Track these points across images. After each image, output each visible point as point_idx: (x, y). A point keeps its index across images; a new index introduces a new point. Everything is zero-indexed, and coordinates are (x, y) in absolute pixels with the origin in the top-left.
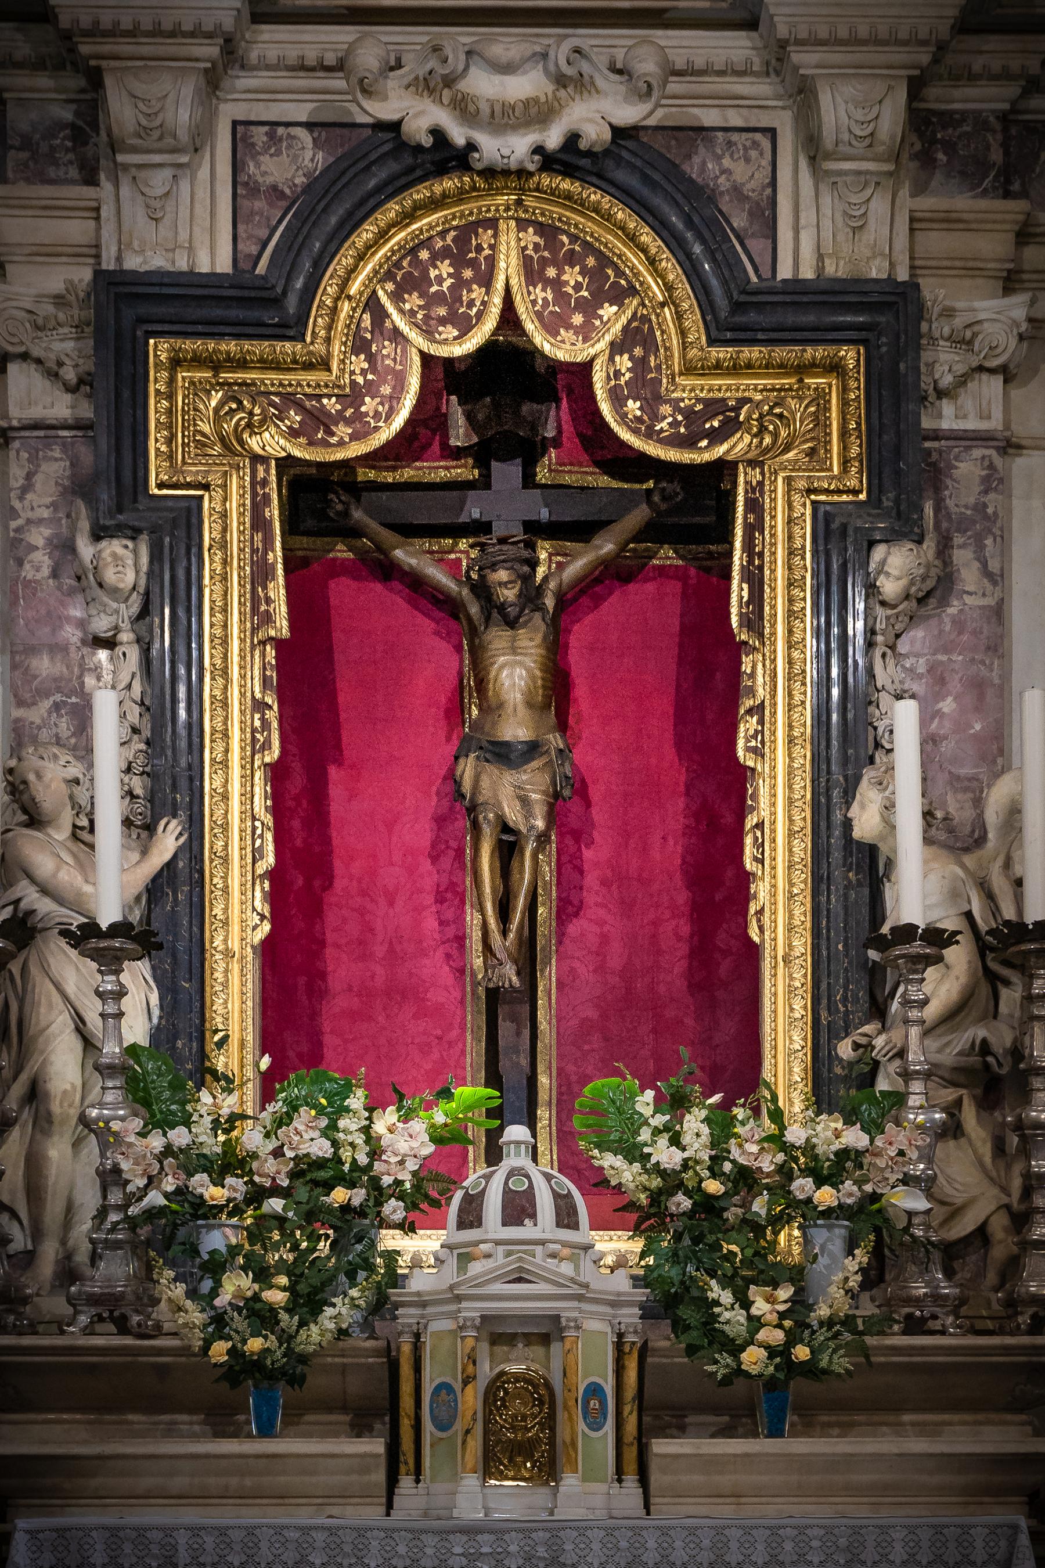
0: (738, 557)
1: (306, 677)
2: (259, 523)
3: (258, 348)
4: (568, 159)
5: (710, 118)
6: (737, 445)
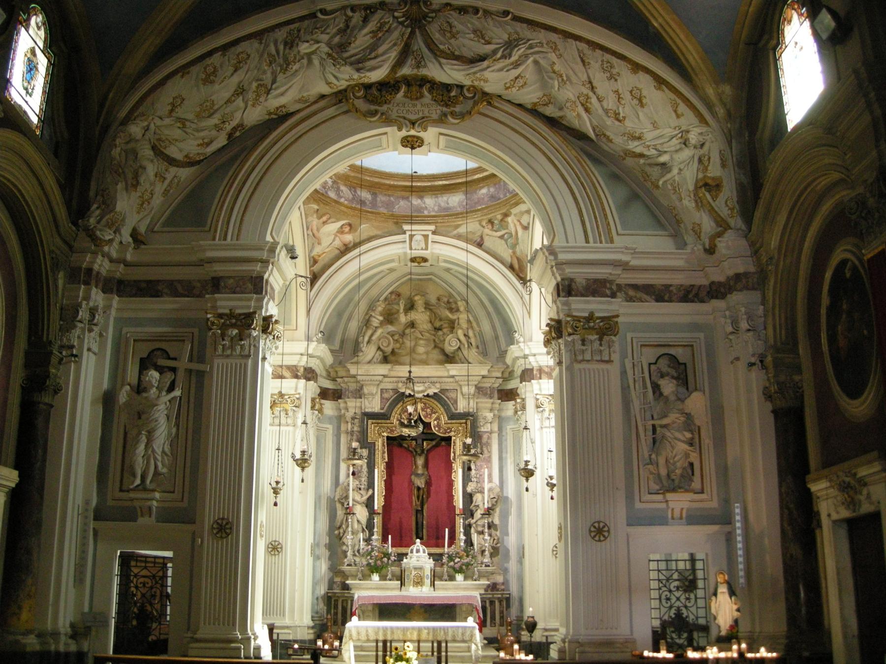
1: (390, 467)
2: (383, 445)
3: (383, 421)
4: (428, 396)
6: (452, 434)
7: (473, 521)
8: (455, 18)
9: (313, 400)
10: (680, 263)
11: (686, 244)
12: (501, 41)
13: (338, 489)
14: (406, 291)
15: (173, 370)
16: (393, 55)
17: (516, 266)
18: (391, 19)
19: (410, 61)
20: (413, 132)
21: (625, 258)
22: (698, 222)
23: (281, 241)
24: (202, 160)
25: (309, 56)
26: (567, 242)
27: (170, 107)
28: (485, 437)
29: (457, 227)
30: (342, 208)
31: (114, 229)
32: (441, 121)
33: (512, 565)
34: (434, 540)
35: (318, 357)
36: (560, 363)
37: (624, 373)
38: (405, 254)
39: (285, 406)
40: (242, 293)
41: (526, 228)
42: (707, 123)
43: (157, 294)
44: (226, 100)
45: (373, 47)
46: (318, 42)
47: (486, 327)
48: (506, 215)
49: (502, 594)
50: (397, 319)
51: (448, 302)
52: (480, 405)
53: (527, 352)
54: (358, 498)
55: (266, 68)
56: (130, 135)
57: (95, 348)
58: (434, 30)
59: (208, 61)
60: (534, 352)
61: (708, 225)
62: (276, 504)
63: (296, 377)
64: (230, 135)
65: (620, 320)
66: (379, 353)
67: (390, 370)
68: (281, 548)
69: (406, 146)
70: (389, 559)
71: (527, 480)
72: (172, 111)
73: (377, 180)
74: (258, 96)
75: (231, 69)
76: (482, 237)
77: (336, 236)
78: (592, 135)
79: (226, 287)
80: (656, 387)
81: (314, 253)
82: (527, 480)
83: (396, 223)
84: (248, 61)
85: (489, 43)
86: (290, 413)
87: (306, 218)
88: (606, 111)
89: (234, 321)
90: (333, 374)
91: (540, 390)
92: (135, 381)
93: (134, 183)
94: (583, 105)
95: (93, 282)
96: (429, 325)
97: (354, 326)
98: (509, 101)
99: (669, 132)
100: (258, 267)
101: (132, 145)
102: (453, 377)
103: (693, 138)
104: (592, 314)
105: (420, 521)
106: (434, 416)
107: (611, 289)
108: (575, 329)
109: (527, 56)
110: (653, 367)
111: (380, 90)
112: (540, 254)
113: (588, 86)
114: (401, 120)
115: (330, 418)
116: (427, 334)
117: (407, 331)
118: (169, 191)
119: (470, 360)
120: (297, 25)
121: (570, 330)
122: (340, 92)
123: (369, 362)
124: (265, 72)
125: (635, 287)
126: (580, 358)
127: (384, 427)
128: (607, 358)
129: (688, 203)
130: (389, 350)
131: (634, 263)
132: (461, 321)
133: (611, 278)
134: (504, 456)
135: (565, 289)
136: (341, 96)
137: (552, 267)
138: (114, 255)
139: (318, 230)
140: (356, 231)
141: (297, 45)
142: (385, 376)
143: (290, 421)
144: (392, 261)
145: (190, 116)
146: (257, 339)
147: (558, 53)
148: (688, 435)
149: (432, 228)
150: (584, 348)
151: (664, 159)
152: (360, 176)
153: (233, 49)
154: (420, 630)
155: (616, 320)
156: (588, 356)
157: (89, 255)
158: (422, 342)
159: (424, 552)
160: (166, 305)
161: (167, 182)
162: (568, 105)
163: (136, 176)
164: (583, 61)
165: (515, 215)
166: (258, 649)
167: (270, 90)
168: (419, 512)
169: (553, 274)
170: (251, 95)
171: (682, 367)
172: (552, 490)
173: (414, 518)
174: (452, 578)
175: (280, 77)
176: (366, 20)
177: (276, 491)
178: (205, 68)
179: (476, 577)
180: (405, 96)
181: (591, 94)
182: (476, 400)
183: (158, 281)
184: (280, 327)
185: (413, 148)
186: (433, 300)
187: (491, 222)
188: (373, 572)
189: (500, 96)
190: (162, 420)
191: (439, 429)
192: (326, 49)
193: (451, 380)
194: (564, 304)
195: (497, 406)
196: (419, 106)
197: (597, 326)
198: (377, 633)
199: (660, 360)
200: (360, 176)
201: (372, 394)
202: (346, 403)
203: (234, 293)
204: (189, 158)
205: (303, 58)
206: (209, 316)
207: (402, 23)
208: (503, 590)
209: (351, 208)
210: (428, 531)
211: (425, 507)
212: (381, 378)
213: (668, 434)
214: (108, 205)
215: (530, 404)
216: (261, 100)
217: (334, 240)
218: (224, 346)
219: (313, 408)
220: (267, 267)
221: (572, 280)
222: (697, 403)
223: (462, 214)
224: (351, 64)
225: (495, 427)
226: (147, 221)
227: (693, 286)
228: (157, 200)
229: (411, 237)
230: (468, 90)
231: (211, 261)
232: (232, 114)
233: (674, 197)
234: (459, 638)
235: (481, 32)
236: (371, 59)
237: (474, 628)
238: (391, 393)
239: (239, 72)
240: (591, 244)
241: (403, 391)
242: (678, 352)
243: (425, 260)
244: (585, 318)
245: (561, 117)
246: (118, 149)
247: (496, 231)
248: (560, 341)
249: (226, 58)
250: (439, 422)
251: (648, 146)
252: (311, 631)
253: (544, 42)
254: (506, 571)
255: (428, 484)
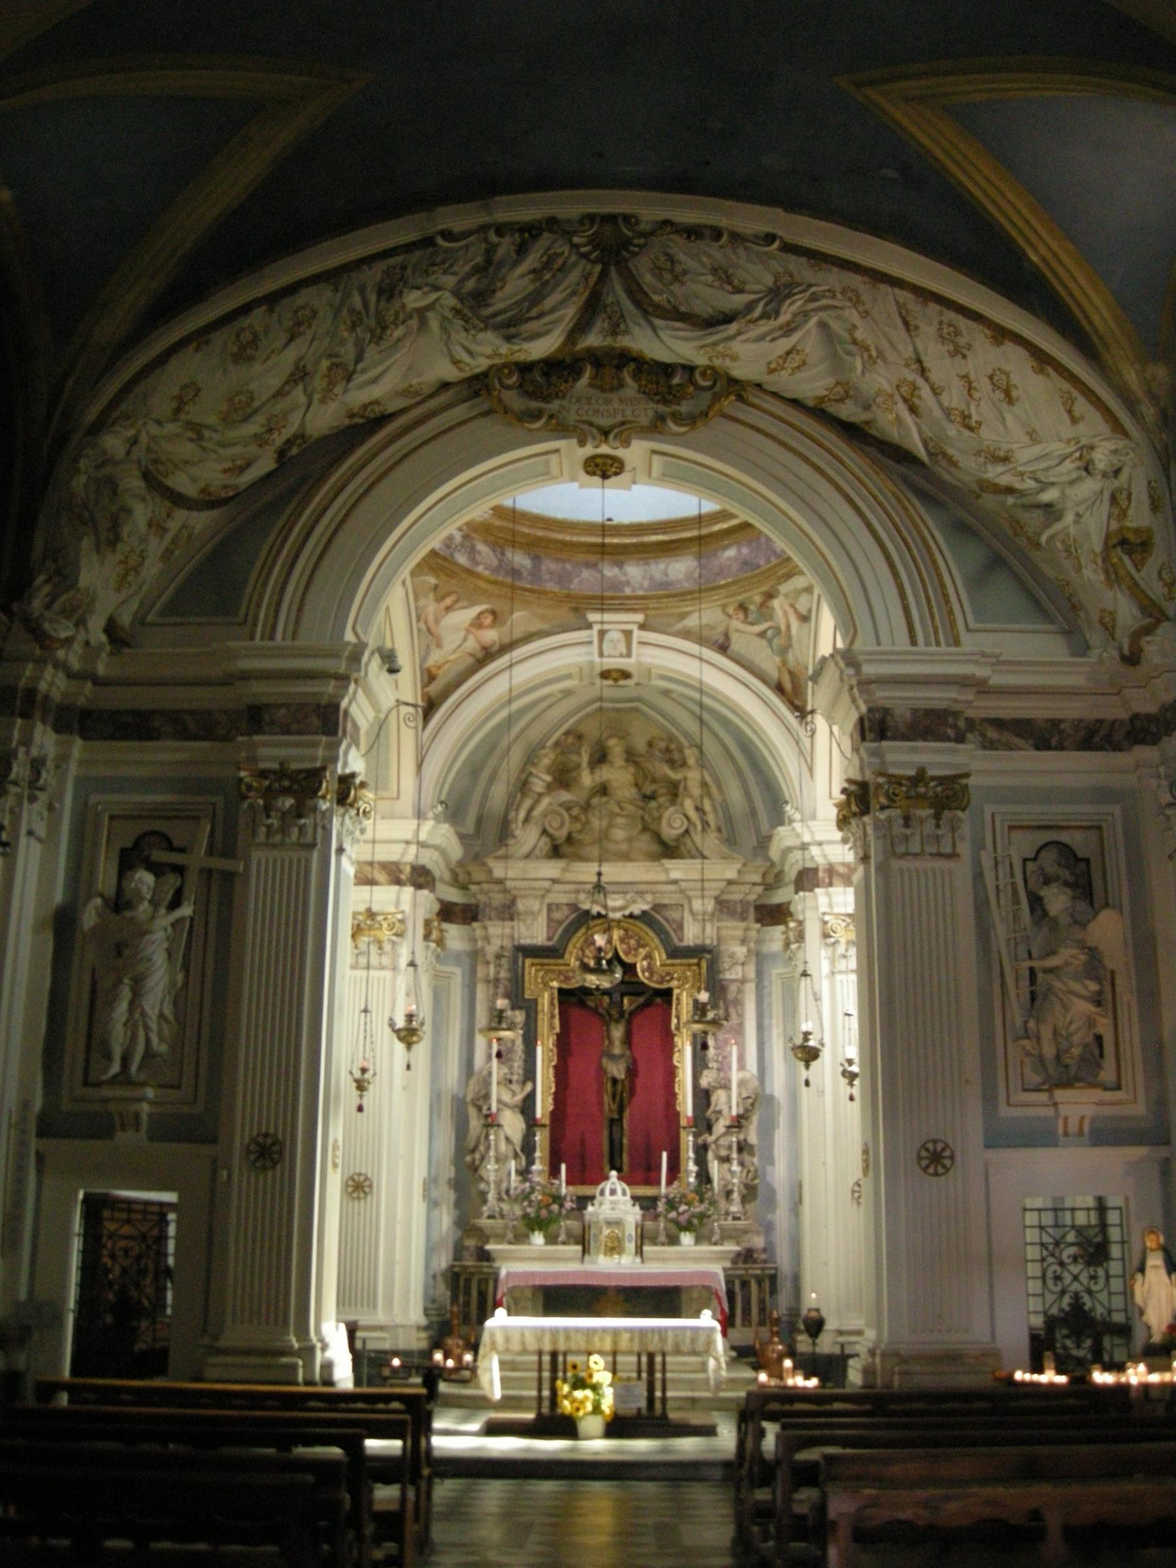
0: (674, 1012)
1: (563, 1044)
2: (552, 1004)
3: (552, 961)
4: (631, 916)
5: (666, 902)
6: (674, 984)
7: (711, 1139)
8: (679, 246)
9: (427, 923)
10: (1076, 680)
11: (1088, 648)
12: (760, 287)
13: (472, 1082)
14: (592, 731)
15: (180, 870)
16: (570, 312)
17: (788, 686)
18: (566, 250)
19: (601, 323)
20: (605, 449)
21: (980, 672)
22: (1110, 608)
23: (372, 642)
24: (232, 498)
25: (421, 312)
26: (879, 644)
27: (175, 405)
28: (733, 989)
29: (683, 616)
30: (481, 583)
31: (75, 617)
32: (656, 428)
33: (781, 1217)
34: (641, 1172)
35: (436, 848)
36: (865, 859)
37: (978, 876)
38: (591, 663)
39: (378, 933)
40: (301, 733)
41: (805, 619)
42: (1125, 433)
43: (149, 734)
44: (273, 390)
45: (535, 298)
46: (436, 288)
47: (735, 794)
48: (770, 596)
49: (763, 1269)
50: (576, 780)
51: (668, 750)
52: (724, 932)
53: (807, 838)
54: (507, 1097)
55: (345, 334)
56: (105, 453)
57: (41, 831)
58: (643, 268)
59: (245, 322)
60: (819, 837)
61: (1127, 613)
62: (360, 1109)
63: (398, 882)
64: (281, 454)
65: (971, 781)
66: (545, 839)
67: (564, 870)
68: (371, 1186)
69: (593, 474)
70: (561, 1206)
71: (807, 1067)
72: (178, 411)
73: (541, 533)
74: (332, 383)
75: (284, 337)
76: (726, 635)
77: (468, 632)
78: (922, 454)
79: (272, 722)
80: (1036, 902)
81: (430, 662)
82: (807, 1067)
83: (576, 610)
84: (315, 323)
85: (739, 291)
86: (387, 947)
87: (416, 599)
88: (947, 412)
89: (286, 783)
90: (462, 877)
91: (831, 905)
92: (111, 891)
93: (112, 538)
94: (905, 400)
95: (38, 714)
96: (634, 790)
97: (499, 792)
98: (775, 394)
99: (1057, 448)
100: (331, 687)
101: (107, 471)
102: (675, 882)
103: (1101, 458)
104: (922, 771)
105: (616, 1137)
106: (642, 952)
107: (955, 727)
108: (892, 798)
109: (805, 315)
110: (1030, 866)
111: (546, 374)
112: (831, 665)
113: (915, 367)
114: (585, 427)
115: (457, 958)
116: (631, 807)
117: (595, 801)
118: (172, 553)
119: (706, 853)
120: (399, 259)
121: (883, 800)
122: (476, 377)
123: (527, 856)
124: (343, 342)
125: (999, 724)
126: (901, 849)
127: (553, 971)
128: (948, 849)
129: (1092, 574)
130: (562, 834)
131: (997, 680)
132: (690, 784)
133: (956, 707)
134: (766, 1022)
135: (875, 728)
136: (477, 386)
137: (851, 688)
138: (75, 664)
139: (437, 621)
140: (505, 622)
141: (401, 293)
142: (554, 881)
143: (386, 961)
144: (568, 676)
145: (212, 420)
146: (327, 816)
147: (861, 308)
148: (1093, 987)
149: (639, 617)
150: (908, 831)
151: (1048, 496)
152: (510, 525)
153: (285, 302)
154: (616, 1332)
155: (964, 781)
156: (915, 847)
157: (30, 666)
158: (620, 821)
159: (624, 1193)
160: (165, 755)
161: (169, 537)
162: (880, 400)
163: (115, 527)
164: (906, 323)
165: (786, 595)
166: (328, 1366)
167: (354, 372)
168: (615, 1123)
169: (854, 700)
170: (318, 383)
171: (1082, 865)
172: (851, 1084)
173: (606, 1133)
174: (673, 1240)
175: (371, 351)
176: (522, 250)
177: (361, 1086)
178: (238, 336)
179: (716, 1238)
180: (591, 385)
181: (920, 382)
182: (717, 924)
183: (154, 712)
184: (368, 794)
185: (605, 476)
186: (640, 745)
187: (743, 607)
188: (533, 1230)
189: (759, 386)
190: (159, 959)
191: (652, 974)
192: (450, 301)
193: (672, 888)
194: (874, 753)
195: (753, 934)
196: (616, 404)
197: (931, 794)
198: (540, 1339)
199: (1044, 854)
200: (510, 525)
201: (532, 913)
202: (485, 928)
203: (288, 732)
204: (210, 494)
205: (411, 317)
206: (243, 774)
207: (585, 256)
208: (765, 1261)
209: (495, 583)
210: (630, 1156)
211: (626, 1114)
212: (547, 884)
213: (1058, 985)
214: (64, 577)
215: (812, 931)
216: (336, 390)
217: (465, 639)
218: (269, 827)
219: (427, 937)
220: (346, 688)
221: (886, 712)
222: (1108, 929)
223: (690, 593)
224: (496, 328)
225: (751, 972)
226: (134, 605)
227: (1100, 721)
228: (152, 569)
229: (602, 633)
230: (703, 374)
231: (246, 676)
232: (285, 415)
233: (1068, 564)
234: (686, 1347)
235: (726, 272)
236: (532, 319)
237: (712, 1329)
238: (566, 911)
239: (299, 341)
240: (921, 647)
241: (586, 906)
242: (1074, 839)
243: (626, 675)
244: (910, 778)
245: (868, 423)
246: (83, 478)
247: (752, 624)
248: (866, 819)
249: (275, 316)
250: (650, 963)
251: (1022, 474)
252: (423, 1335)
253: (838, 289)
254: (769, 1228)
255: (632, 1072)
